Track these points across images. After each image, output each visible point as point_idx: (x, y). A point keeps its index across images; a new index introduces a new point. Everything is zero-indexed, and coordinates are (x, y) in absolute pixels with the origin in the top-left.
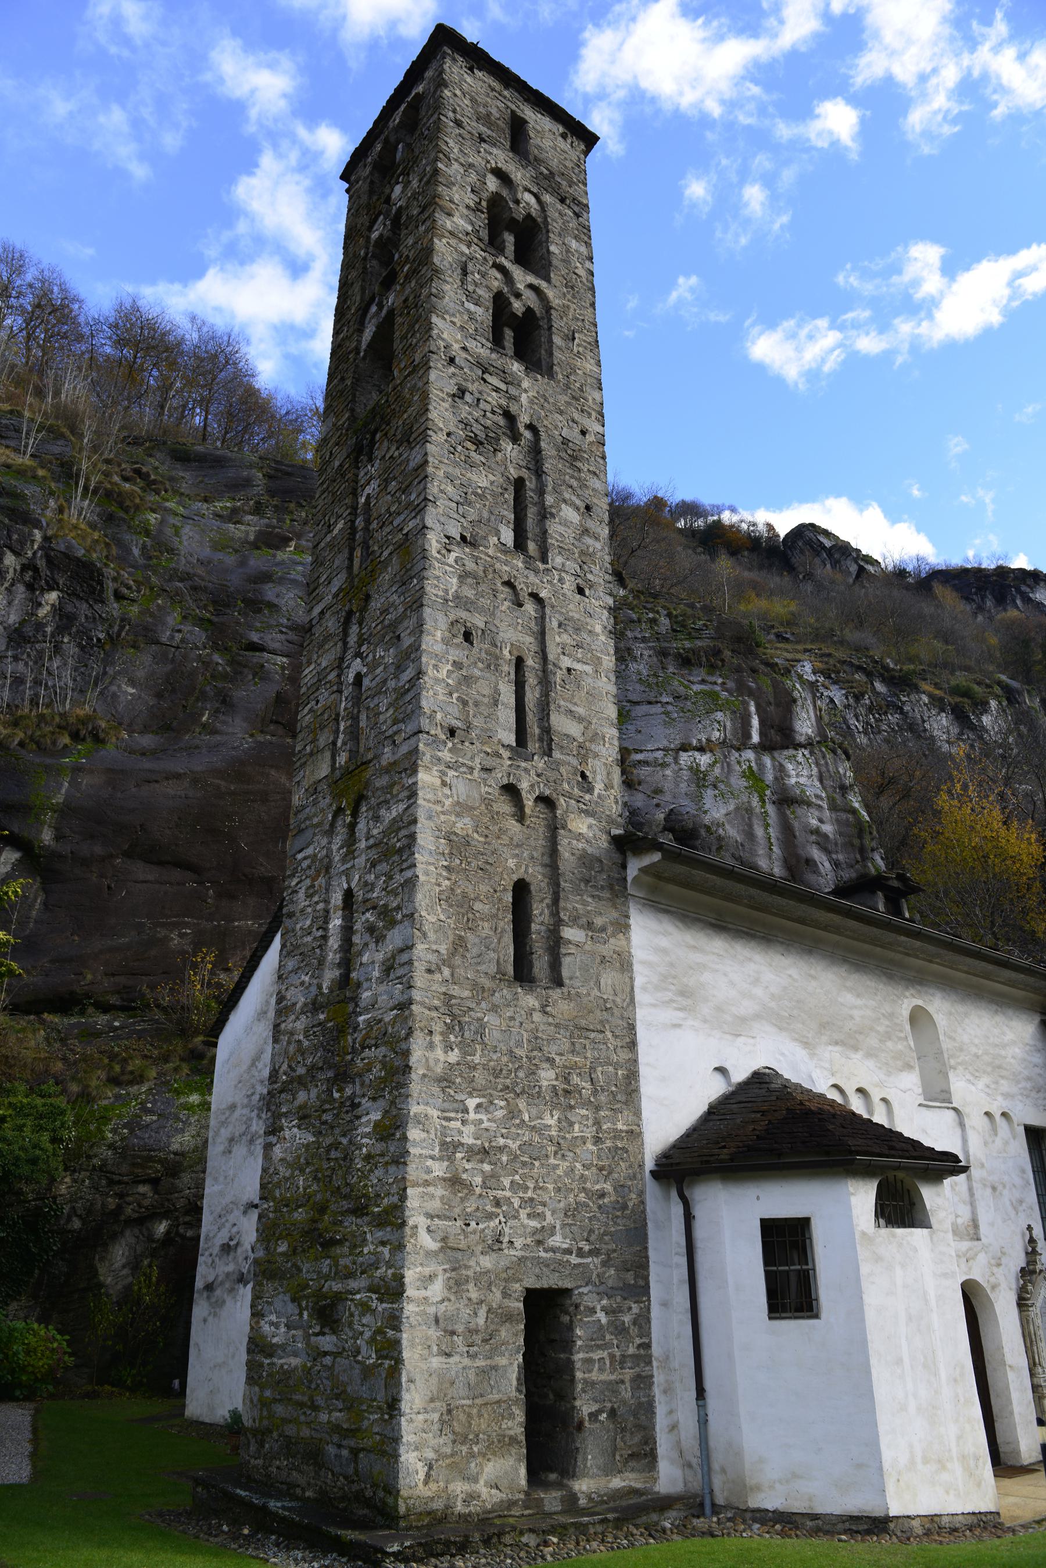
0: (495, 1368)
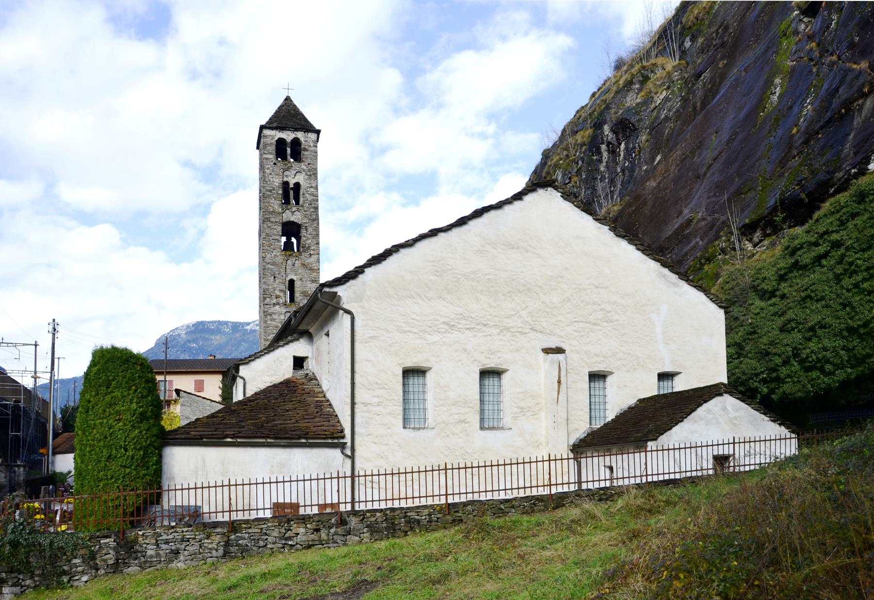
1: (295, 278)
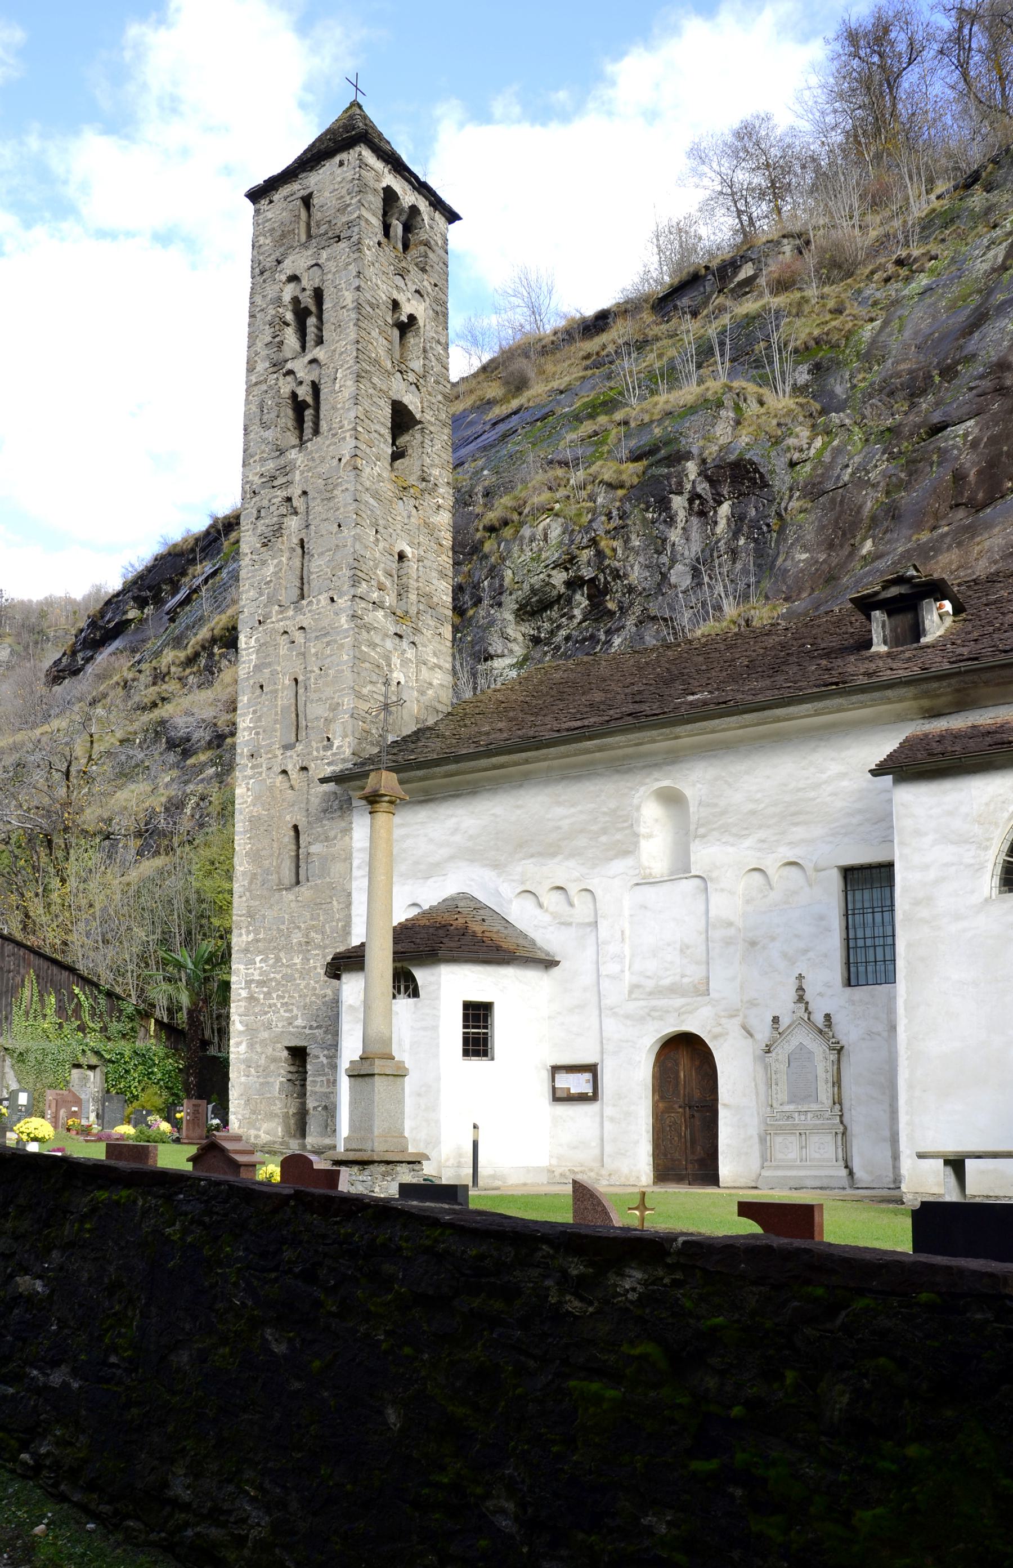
0: (268, 1083)
1: (409, 551)
